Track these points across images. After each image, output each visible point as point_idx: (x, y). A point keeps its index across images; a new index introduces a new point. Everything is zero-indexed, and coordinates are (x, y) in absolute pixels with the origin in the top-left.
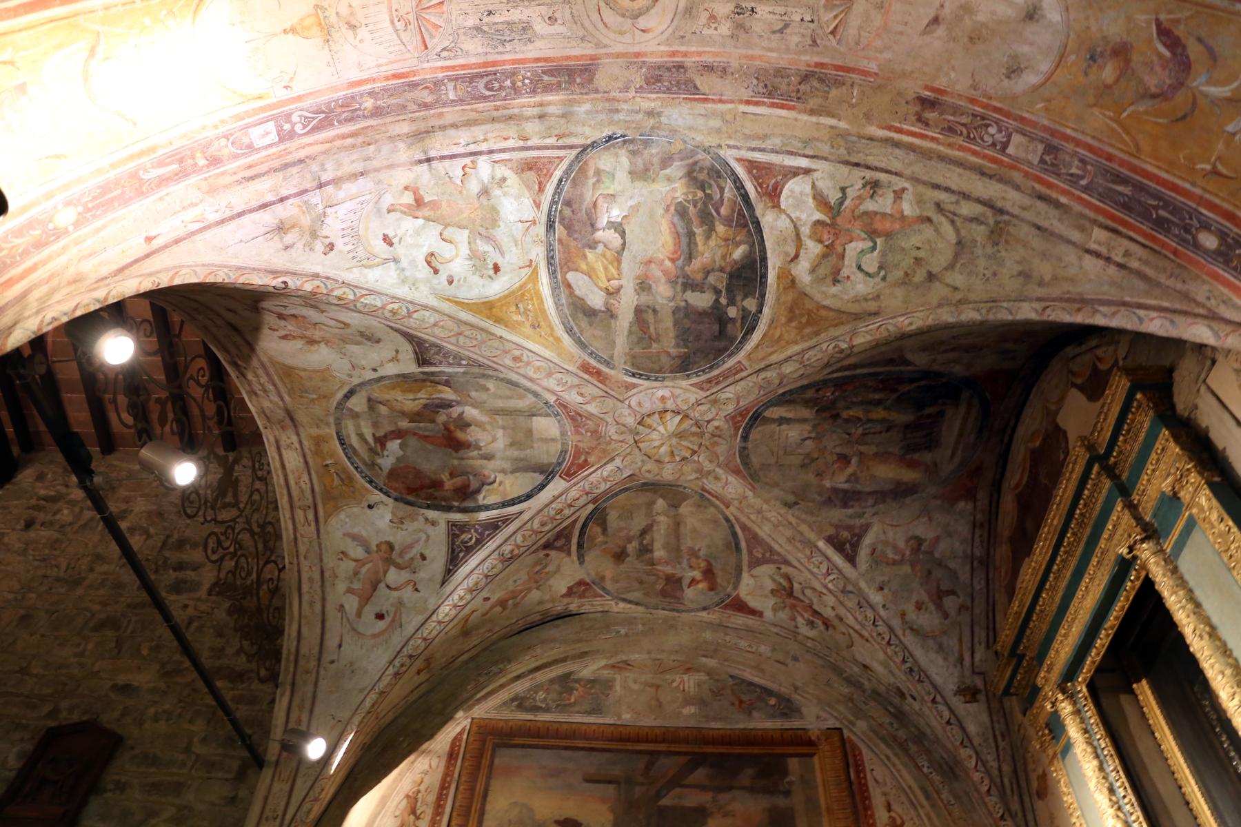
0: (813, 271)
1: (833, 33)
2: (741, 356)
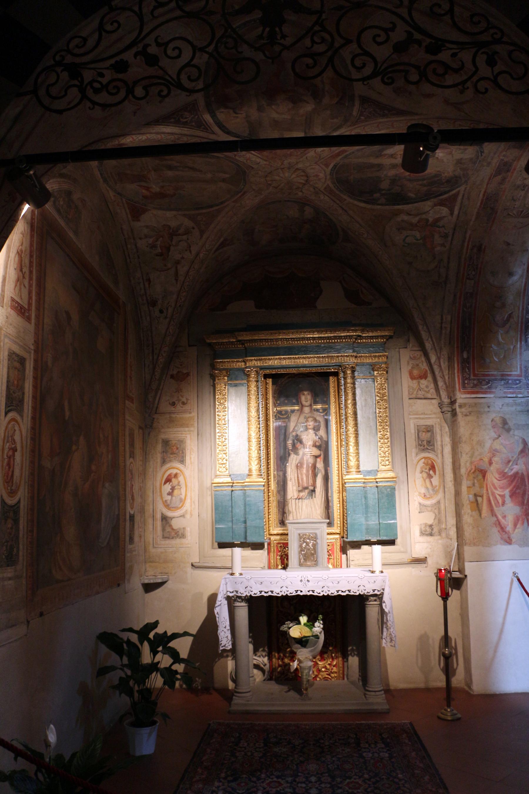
0: (403, 221)
1: (509, 214)
2: (349, 200)
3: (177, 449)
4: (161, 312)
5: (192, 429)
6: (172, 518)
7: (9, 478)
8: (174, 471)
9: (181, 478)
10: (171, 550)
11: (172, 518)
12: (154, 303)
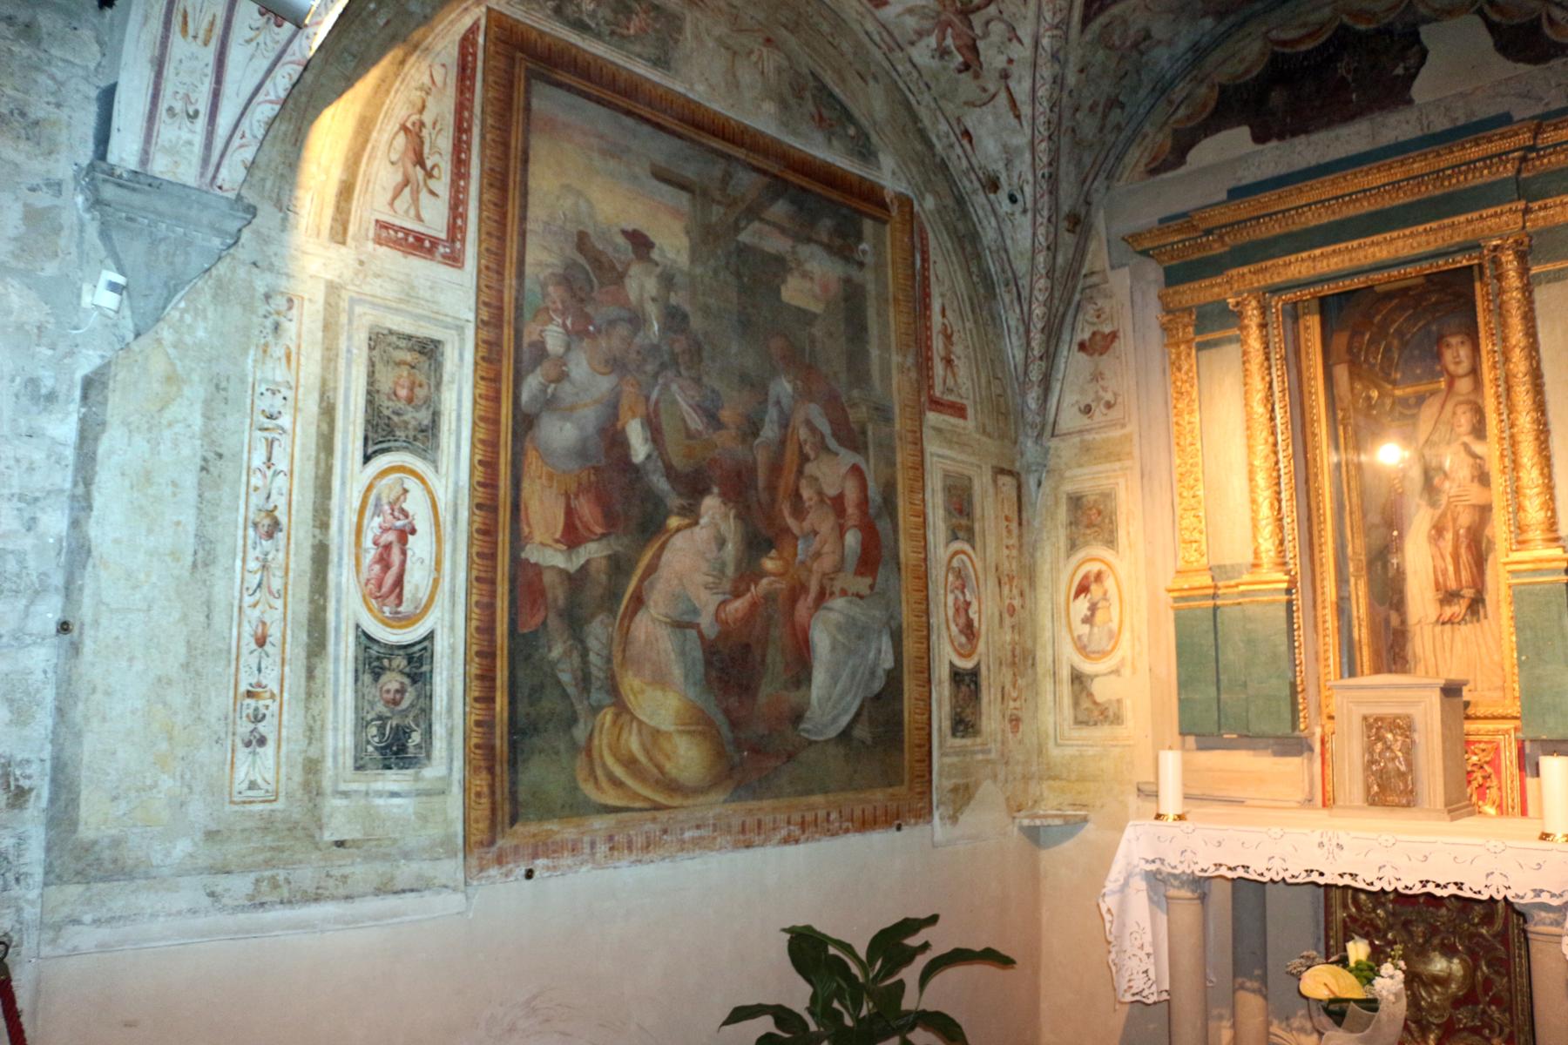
3: (1099, 513)
4: (1013, 199)
5: (1128, 463)
6: (1092, 677)
7: (385, 589)
8: (1094, 567)
9: (1109, 583)
10: (1091, 752)
11: (1092, 677)
12: (993, 185)
